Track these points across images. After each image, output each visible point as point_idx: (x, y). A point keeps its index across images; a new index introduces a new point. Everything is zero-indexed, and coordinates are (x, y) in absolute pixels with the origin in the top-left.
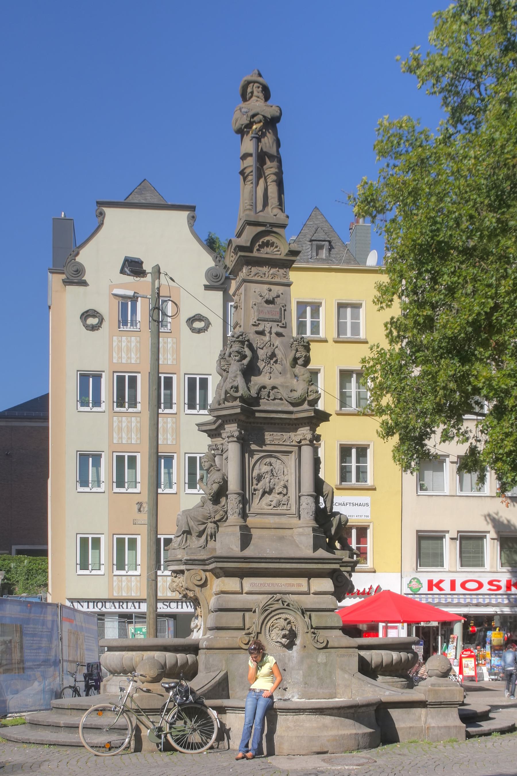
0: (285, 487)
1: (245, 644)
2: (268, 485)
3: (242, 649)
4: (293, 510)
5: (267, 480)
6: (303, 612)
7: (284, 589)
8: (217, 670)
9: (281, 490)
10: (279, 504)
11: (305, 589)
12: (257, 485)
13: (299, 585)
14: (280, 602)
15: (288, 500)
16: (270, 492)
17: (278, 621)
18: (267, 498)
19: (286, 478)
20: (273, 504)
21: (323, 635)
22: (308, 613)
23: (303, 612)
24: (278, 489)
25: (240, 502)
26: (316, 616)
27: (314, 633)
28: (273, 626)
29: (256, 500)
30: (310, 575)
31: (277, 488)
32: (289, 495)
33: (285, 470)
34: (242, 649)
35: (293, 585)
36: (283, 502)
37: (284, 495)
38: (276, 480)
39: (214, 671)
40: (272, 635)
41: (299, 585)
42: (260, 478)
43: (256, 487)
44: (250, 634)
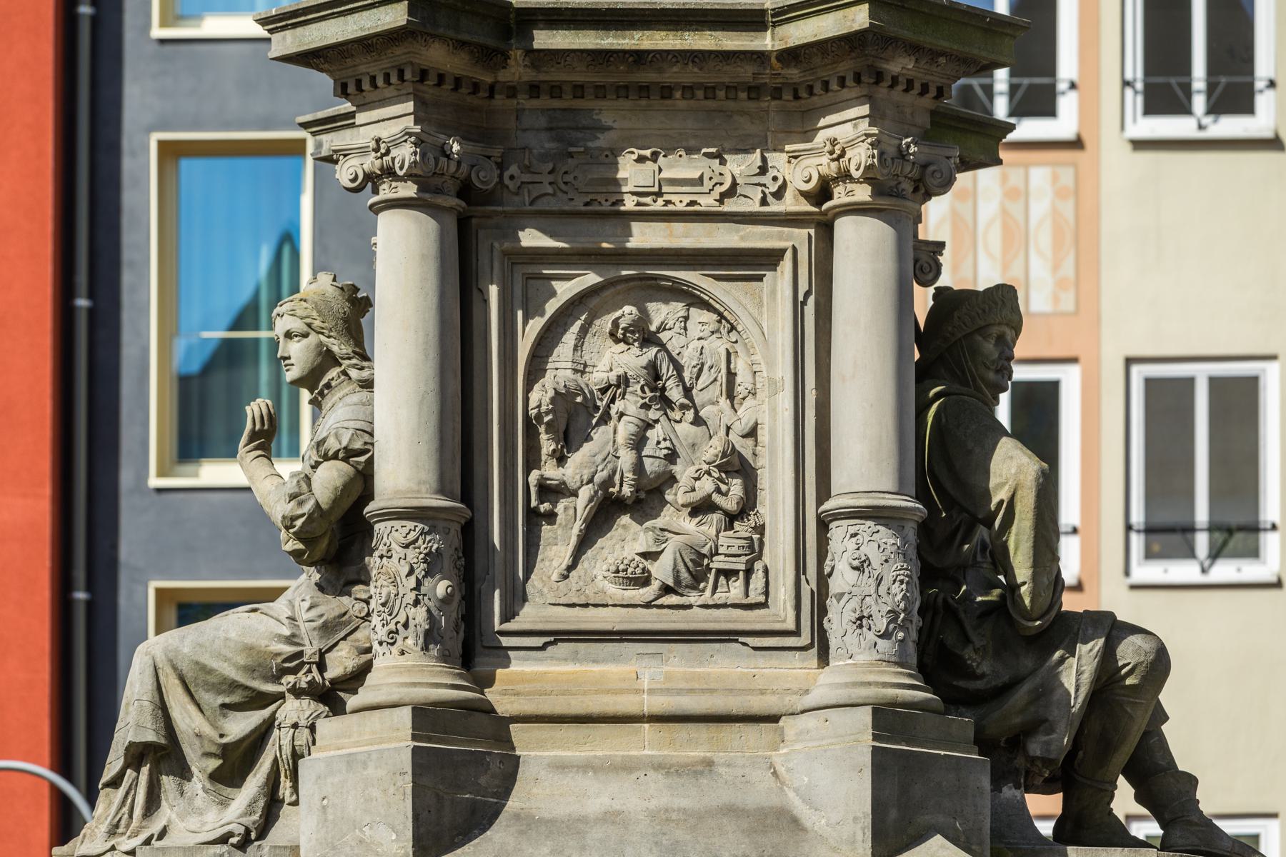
0: (736, 466)
2: (626, 459)
4: (782, 611)
5: (625, 429)
9: (706, 485)
10: (697, 569)
12: (561, 460)
15: (754, 550)
16: (647, 498)
18: (627, 539)
19: (746, 414)
20: (662, 571)
24: (692, 480)
25: (433, 564)
29: (556, 546)
31: (684, 472)
32: (764, 509)
33: (740, 366)
36: (719, 563)
37: (731, 519)
38: (685, 429)
42: (575, 418)
43: (550, 471)
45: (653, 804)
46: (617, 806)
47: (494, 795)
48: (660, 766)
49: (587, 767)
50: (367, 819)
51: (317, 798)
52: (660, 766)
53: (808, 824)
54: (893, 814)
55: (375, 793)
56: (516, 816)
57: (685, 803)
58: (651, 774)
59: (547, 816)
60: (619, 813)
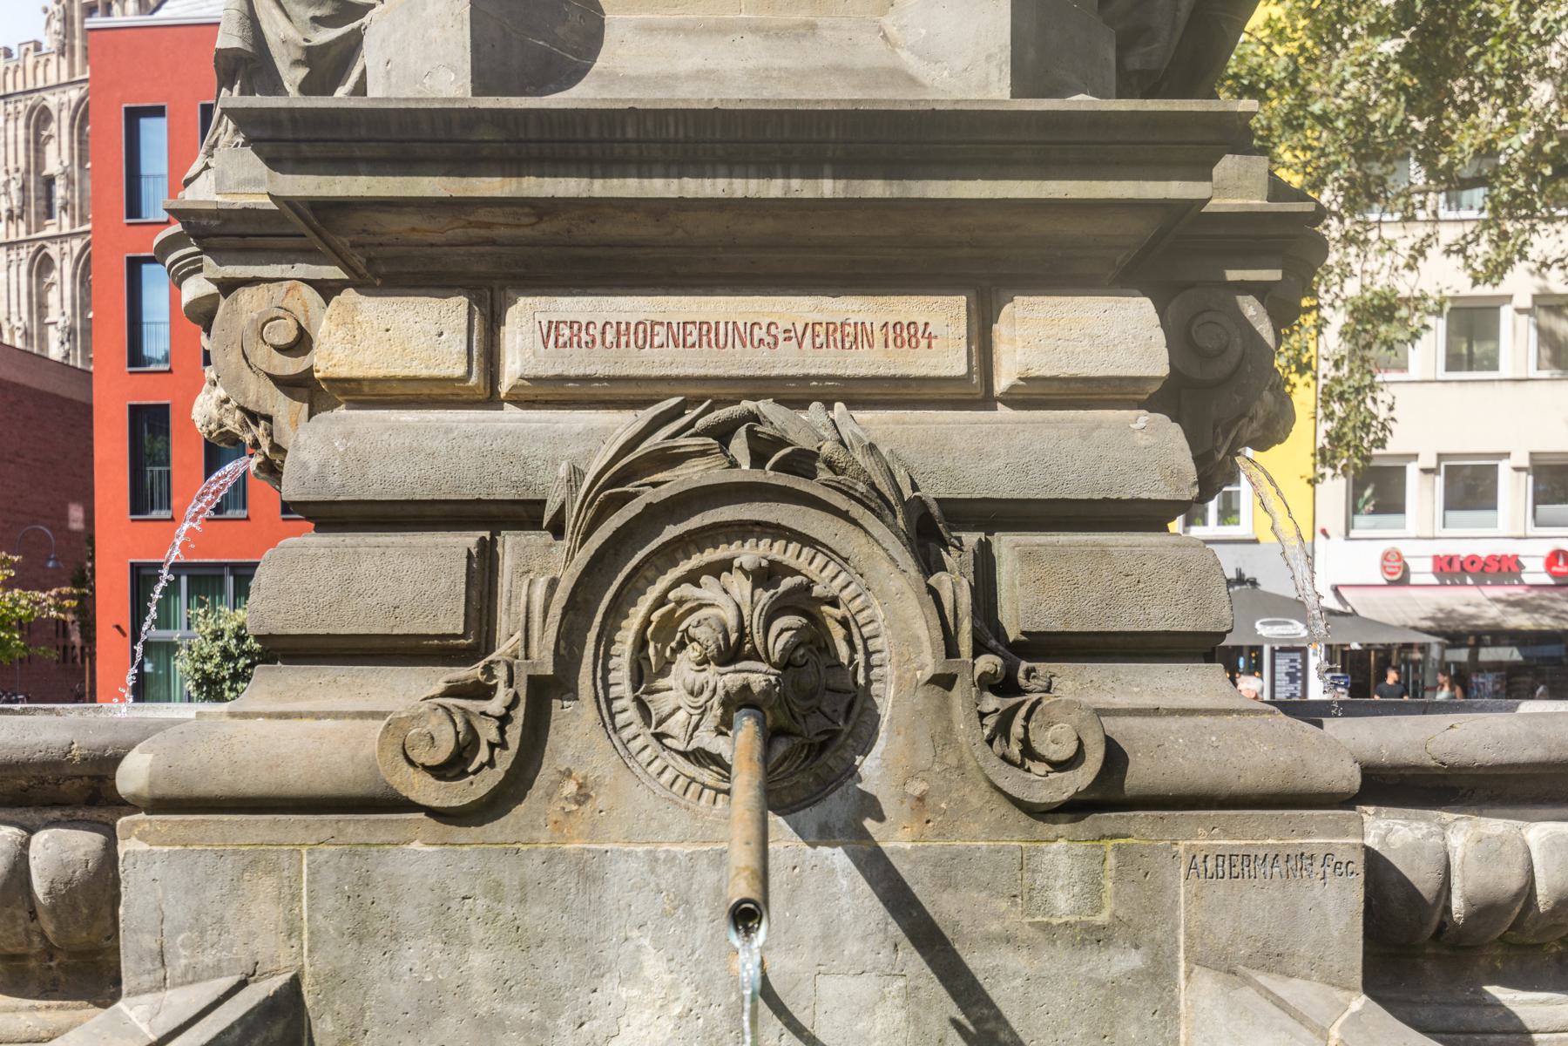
1: (440, 772)
3: (408, 806)
6: (928, 529)
7: (788, 361)
8: (217, 971)
11: (947, 357)
13: (907, 335)
14: (739, 446)
17: (709, 589)
21: (1076, 693)
22: (971, 539)
23: (928, 529)
26: (1028, 556)
27: (1004, 685)
28: (669, 625)
30: (989, 266)
34: (408, 806)
35: (861, 335)
39: (192, 977)
40: (660, 704)
41: (907, 335)
44: (483, 691)
45: (751, 64)
46: (711, 65)
47: (575, 53)
48: (757, 29)
49: (677, 30)
50: (428, 67)
51: (383, 63)
52: (757, 29)
53: (927, 81)
54: (1031, 54)
55: (434, 33)
56: (599, 74)
57: (786, 63)
58: (749, 37)
59: (632, 73)
60: (712, 72)
